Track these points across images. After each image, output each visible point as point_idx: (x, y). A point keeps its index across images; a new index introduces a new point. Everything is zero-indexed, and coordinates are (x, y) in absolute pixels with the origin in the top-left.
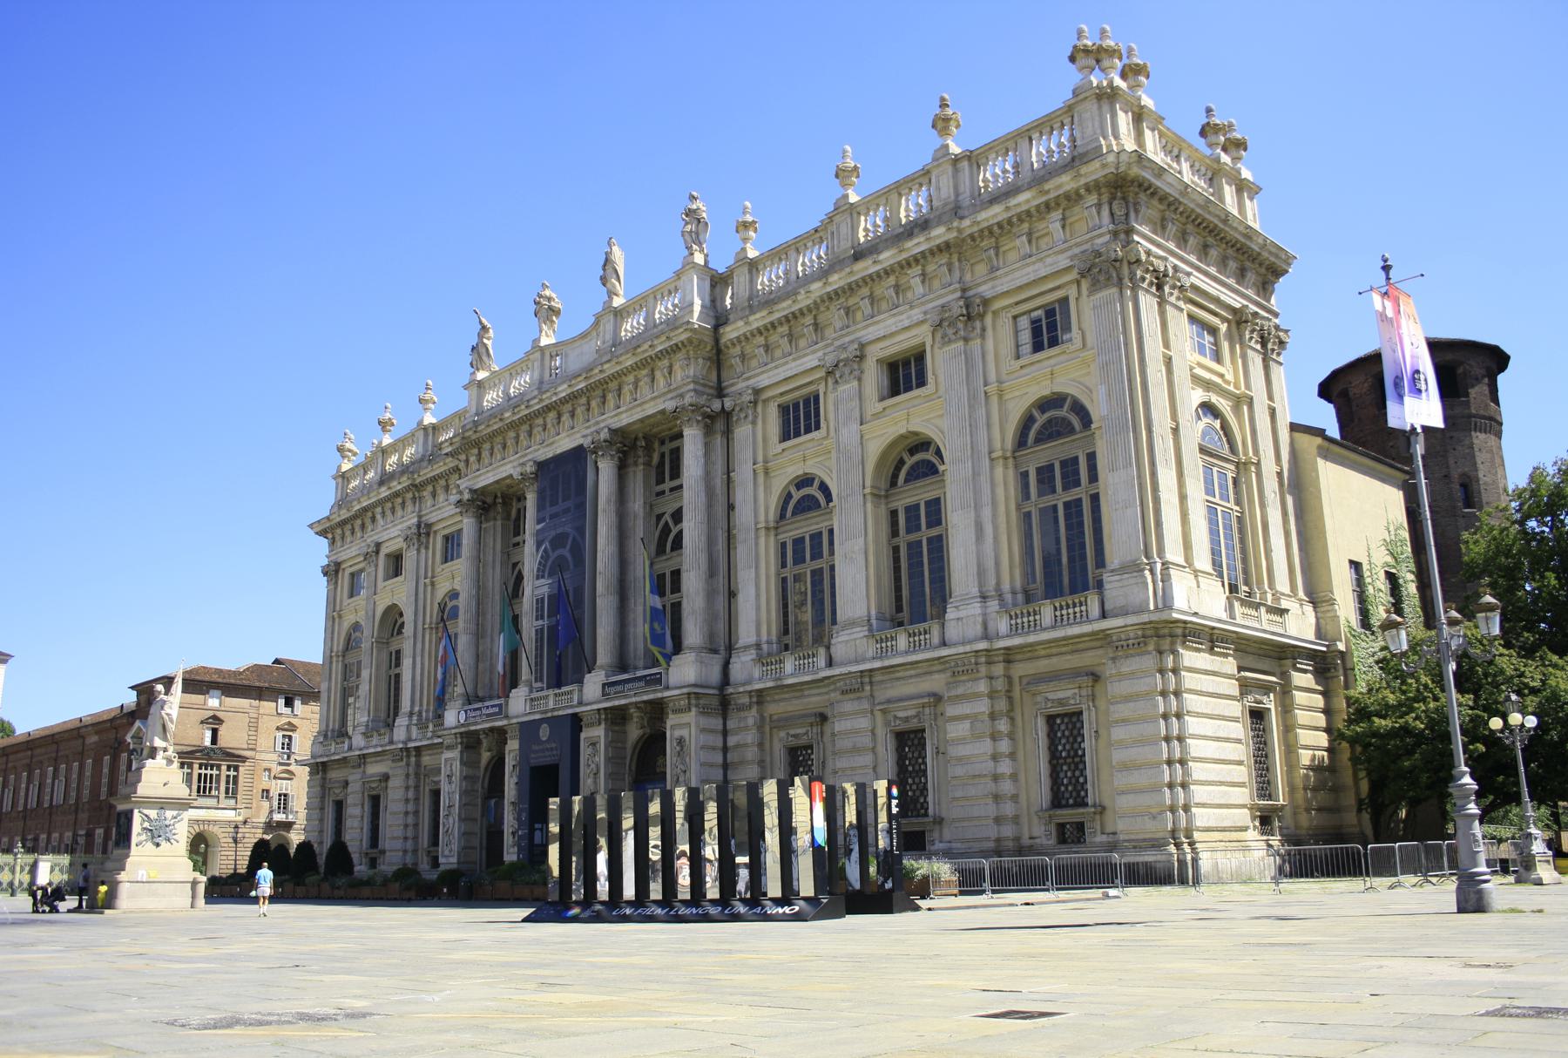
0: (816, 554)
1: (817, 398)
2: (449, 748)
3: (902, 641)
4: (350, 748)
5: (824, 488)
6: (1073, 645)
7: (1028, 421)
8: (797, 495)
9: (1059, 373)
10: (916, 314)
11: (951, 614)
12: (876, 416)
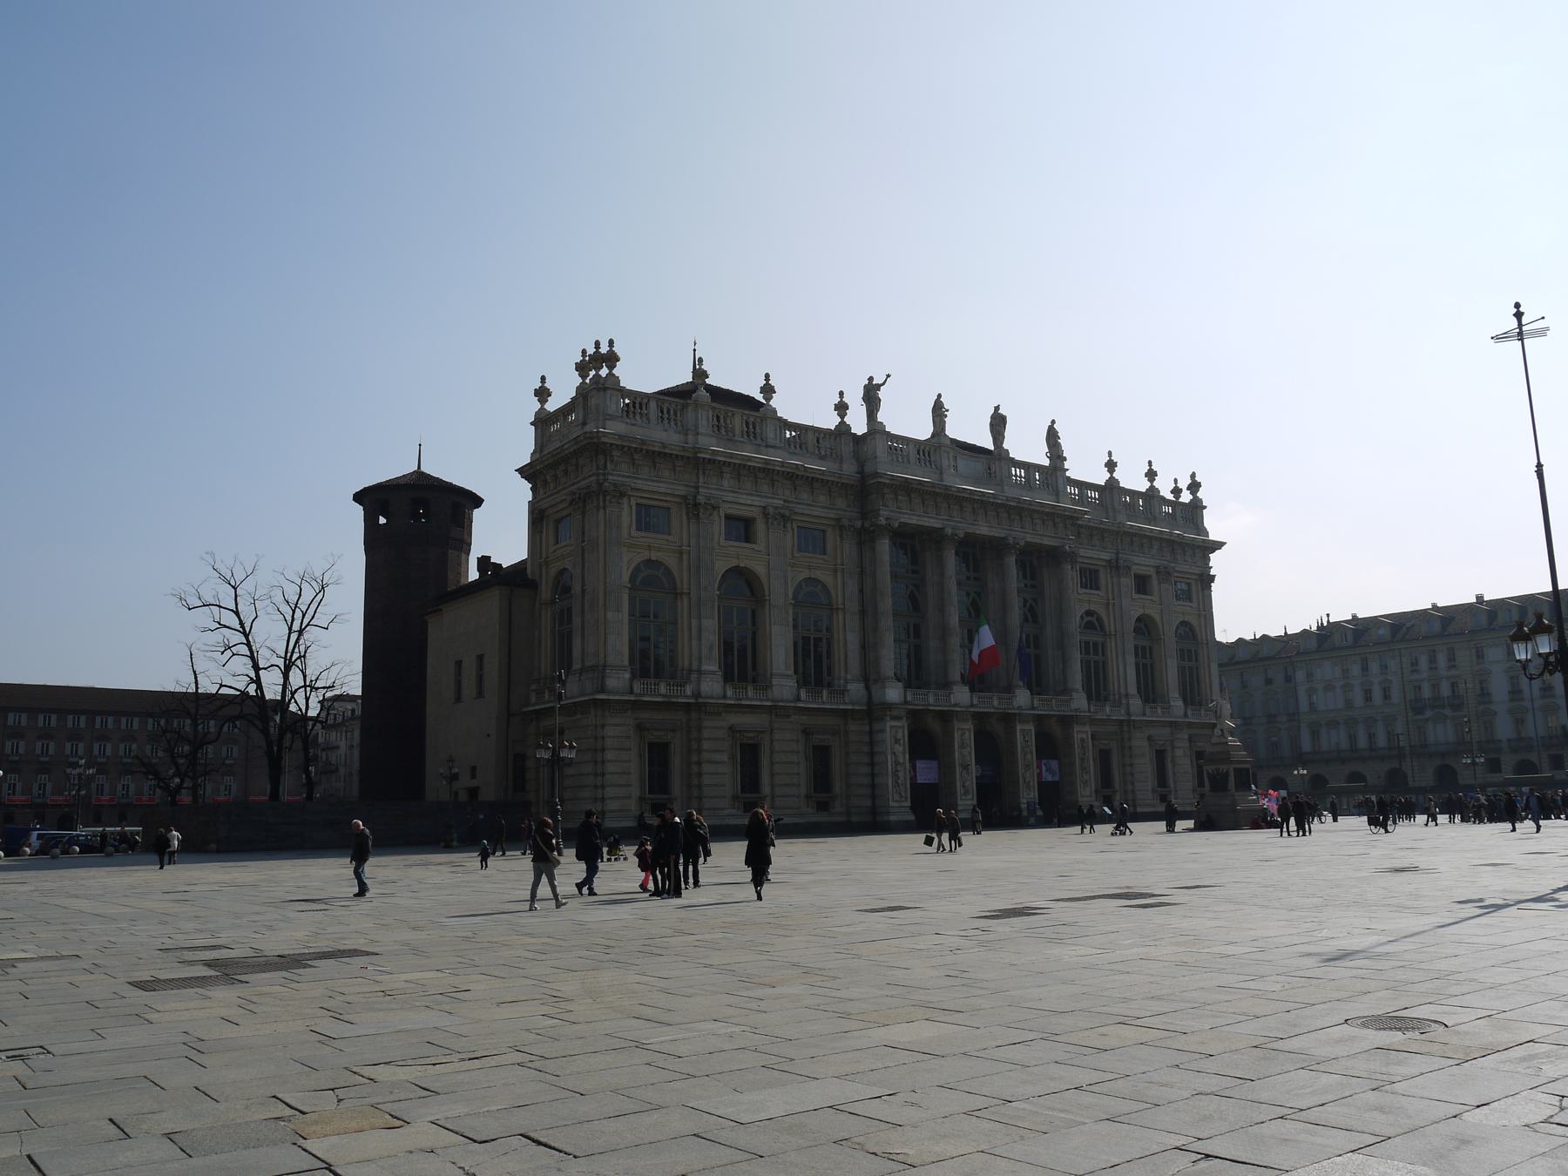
5: (1099, 619)
8: (1087, 619)
10: (1153, 562)
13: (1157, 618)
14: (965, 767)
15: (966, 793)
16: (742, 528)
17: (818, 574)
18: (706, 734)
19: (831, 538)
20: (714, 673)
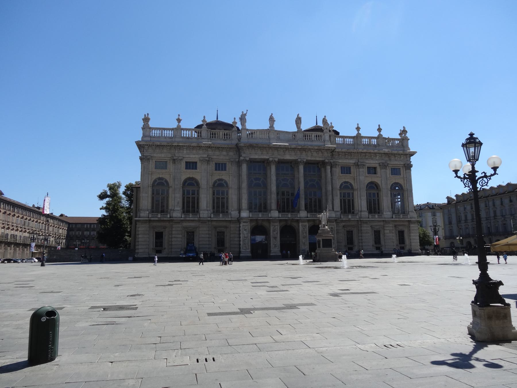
0: (349, 196)
1: (350, 168)
2: (244, 222)
3: (376, 216)
4: (170, 217)
5: (351, 184)
6: (403, 221)
7: (392, 185)
8: (344, 185)
9: (398, 179)
10: (377, 162)
11: (384, 213)
12: (367, 177)
13: (379, 182)
14: (275, 238)
15: (275, 246)
16: (191, 165)
17: (223, 177)
18: (173, 229)
19: (228, 166)
20: (178, 210)
